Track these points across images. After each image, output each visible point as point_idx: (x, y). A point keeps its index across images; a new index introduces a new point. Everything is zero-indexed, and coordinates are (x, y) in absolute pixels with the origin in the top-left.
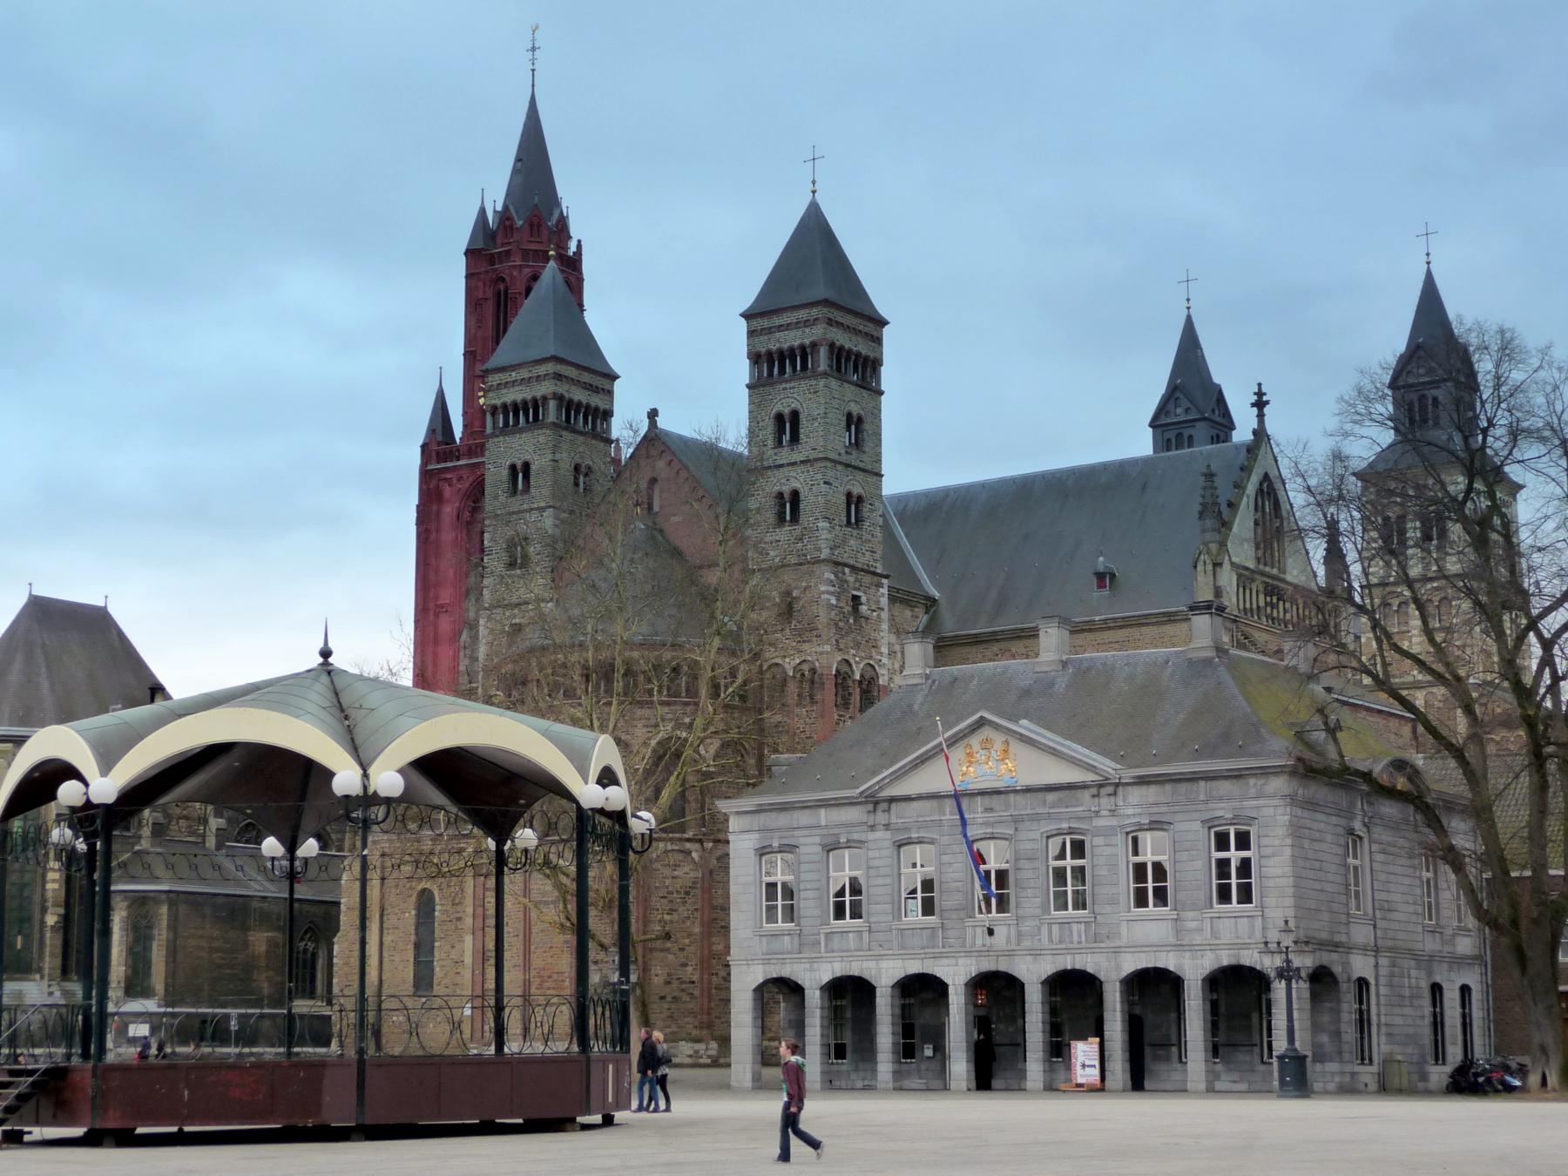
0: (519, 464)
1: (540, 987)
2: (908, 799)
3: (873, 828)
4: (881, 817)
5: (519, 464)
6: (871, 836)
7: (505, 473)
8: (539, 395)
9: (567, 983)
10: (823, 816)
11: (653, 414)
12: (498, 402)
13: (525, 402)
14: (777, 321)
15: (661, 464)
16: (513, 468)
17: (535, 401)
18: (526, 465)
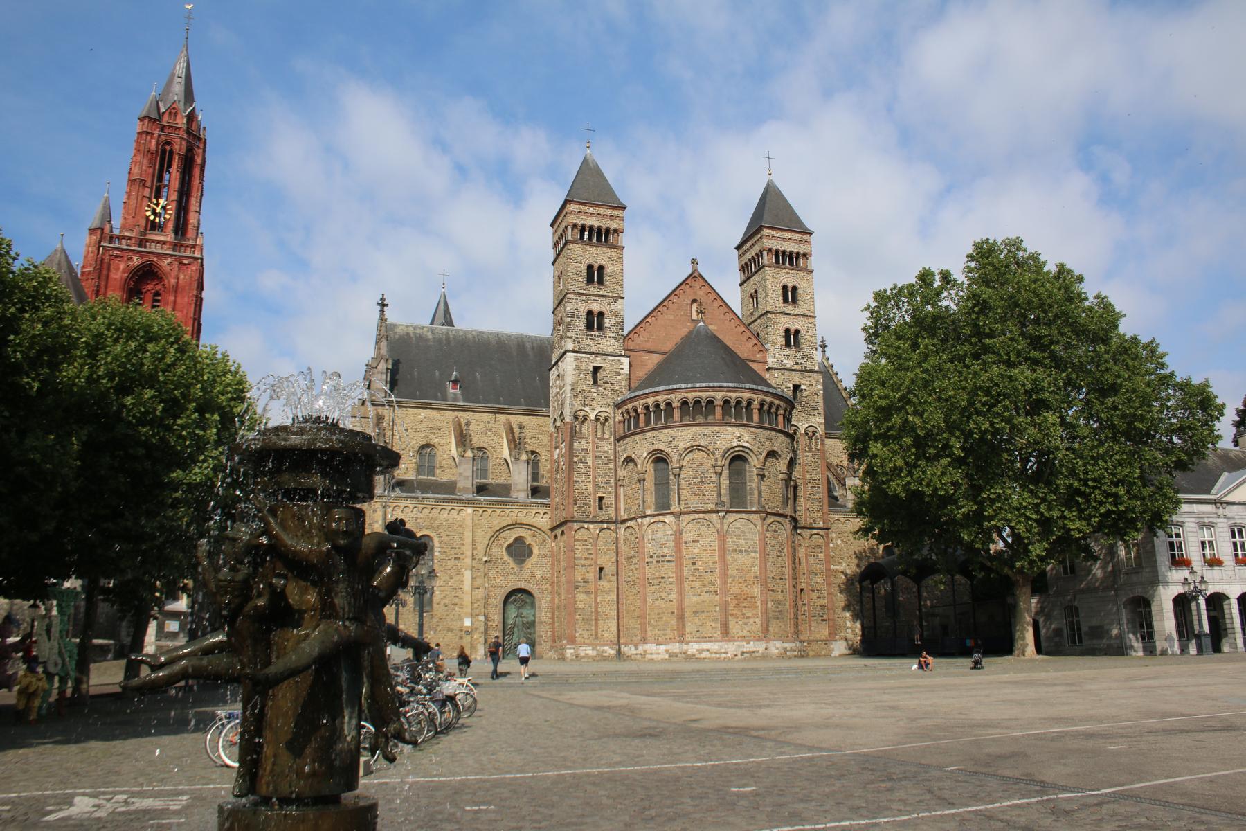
0: (596, 267)
1: (737, 605)
2: (1233, 503)
3: (1219, 516)
4: (1221, 511)
5: (596, 267)
6: (1219, 520)
7: (585, 268)
8: (612, 227)
9: (759, 604)
10: (1196, 508)
11: (694, 262)
12: (580, 223)
13: (599, 229)
14: (780, 234)
15: (701, 292)
16: (590, 267)
17: (607, 230)
18: (601, 268)
